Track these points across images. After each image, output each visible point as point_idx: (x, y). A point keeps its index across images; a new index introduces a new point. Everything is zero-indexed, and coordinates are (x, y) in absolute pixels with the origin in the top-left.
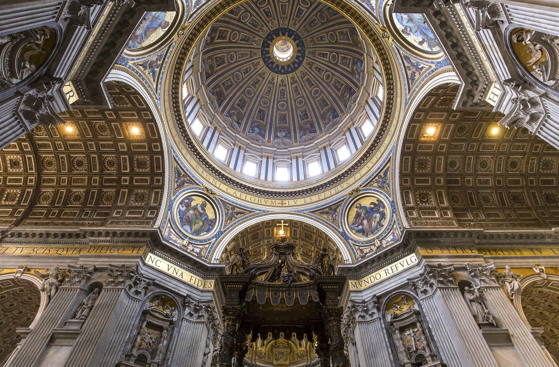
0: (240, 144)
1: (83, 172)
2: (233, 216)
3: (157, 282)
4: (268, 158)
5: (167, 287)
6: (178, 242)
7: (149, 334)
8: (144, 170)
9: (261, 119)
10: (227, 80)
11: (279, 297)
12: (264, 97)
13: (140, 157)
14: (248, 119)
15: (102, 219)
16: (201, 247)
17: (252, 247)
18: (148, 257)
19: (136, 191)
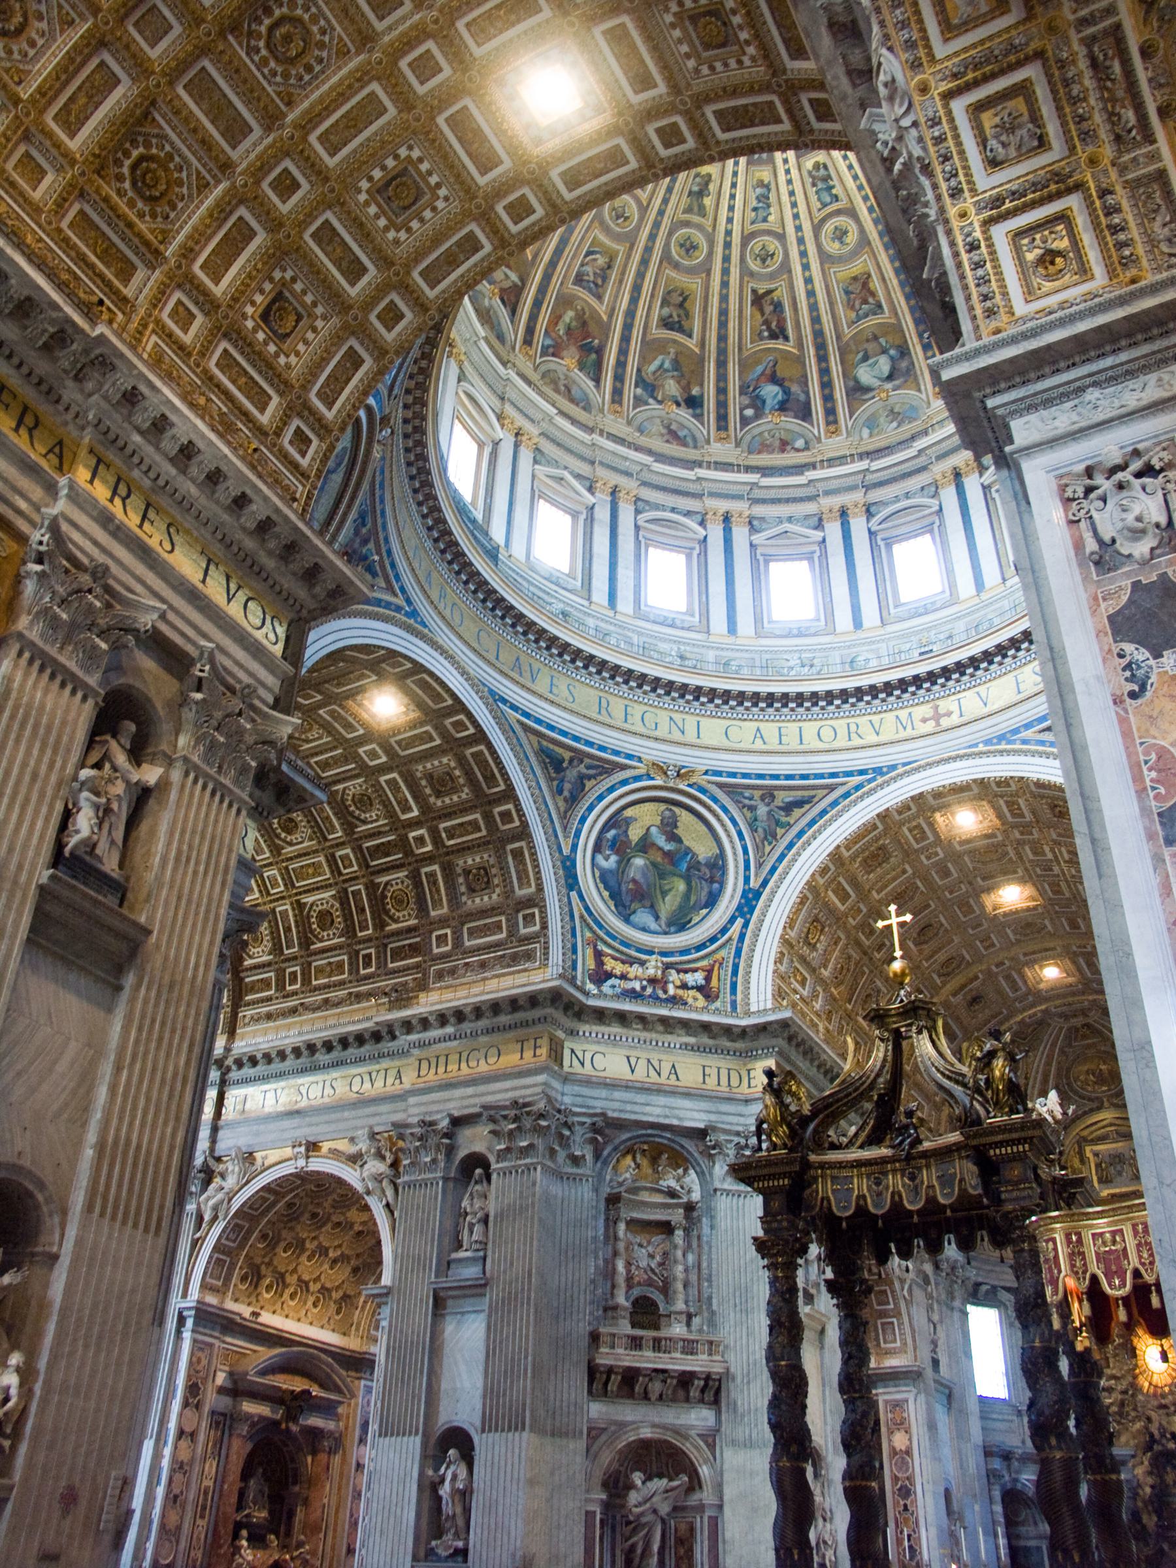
0: (723, 506)
1: (305, 844)
2: (778, 823)
3: (615, 1115)
4: (843, 513)
5: (645, 1119)
6: (631, 976)
7: (640, 1245)
8: (455, 798)
9: (773, 336)
10: (586, 255)
11: (887, 1188)
12: (753, 235)
13: (429, 766)
14: (722, 364)
15: (407, 968)
16: (704, 963)
17: (878, 892)
18: (567, 1052)
19: (461, 862)
